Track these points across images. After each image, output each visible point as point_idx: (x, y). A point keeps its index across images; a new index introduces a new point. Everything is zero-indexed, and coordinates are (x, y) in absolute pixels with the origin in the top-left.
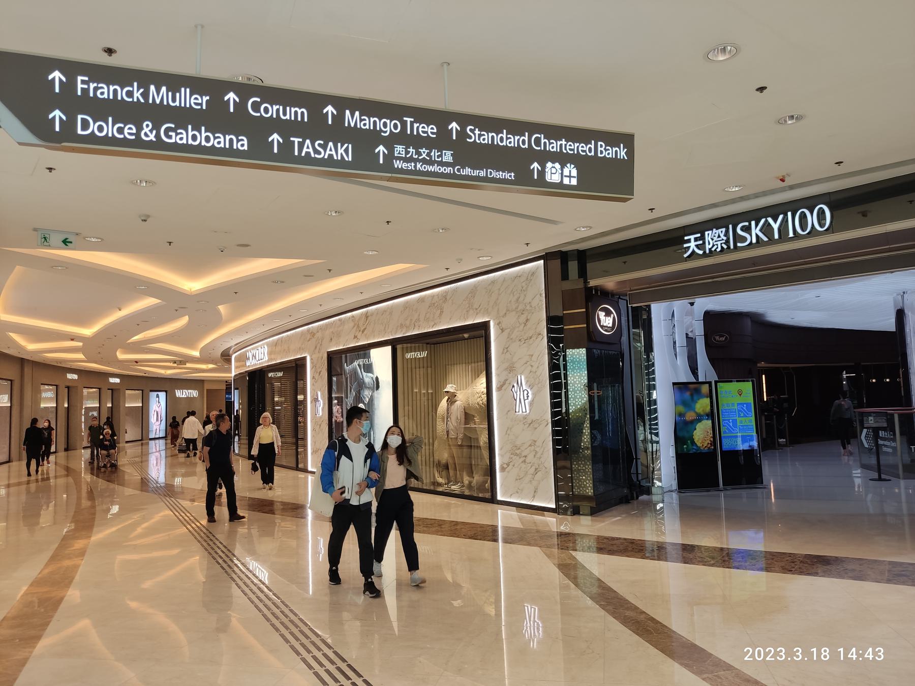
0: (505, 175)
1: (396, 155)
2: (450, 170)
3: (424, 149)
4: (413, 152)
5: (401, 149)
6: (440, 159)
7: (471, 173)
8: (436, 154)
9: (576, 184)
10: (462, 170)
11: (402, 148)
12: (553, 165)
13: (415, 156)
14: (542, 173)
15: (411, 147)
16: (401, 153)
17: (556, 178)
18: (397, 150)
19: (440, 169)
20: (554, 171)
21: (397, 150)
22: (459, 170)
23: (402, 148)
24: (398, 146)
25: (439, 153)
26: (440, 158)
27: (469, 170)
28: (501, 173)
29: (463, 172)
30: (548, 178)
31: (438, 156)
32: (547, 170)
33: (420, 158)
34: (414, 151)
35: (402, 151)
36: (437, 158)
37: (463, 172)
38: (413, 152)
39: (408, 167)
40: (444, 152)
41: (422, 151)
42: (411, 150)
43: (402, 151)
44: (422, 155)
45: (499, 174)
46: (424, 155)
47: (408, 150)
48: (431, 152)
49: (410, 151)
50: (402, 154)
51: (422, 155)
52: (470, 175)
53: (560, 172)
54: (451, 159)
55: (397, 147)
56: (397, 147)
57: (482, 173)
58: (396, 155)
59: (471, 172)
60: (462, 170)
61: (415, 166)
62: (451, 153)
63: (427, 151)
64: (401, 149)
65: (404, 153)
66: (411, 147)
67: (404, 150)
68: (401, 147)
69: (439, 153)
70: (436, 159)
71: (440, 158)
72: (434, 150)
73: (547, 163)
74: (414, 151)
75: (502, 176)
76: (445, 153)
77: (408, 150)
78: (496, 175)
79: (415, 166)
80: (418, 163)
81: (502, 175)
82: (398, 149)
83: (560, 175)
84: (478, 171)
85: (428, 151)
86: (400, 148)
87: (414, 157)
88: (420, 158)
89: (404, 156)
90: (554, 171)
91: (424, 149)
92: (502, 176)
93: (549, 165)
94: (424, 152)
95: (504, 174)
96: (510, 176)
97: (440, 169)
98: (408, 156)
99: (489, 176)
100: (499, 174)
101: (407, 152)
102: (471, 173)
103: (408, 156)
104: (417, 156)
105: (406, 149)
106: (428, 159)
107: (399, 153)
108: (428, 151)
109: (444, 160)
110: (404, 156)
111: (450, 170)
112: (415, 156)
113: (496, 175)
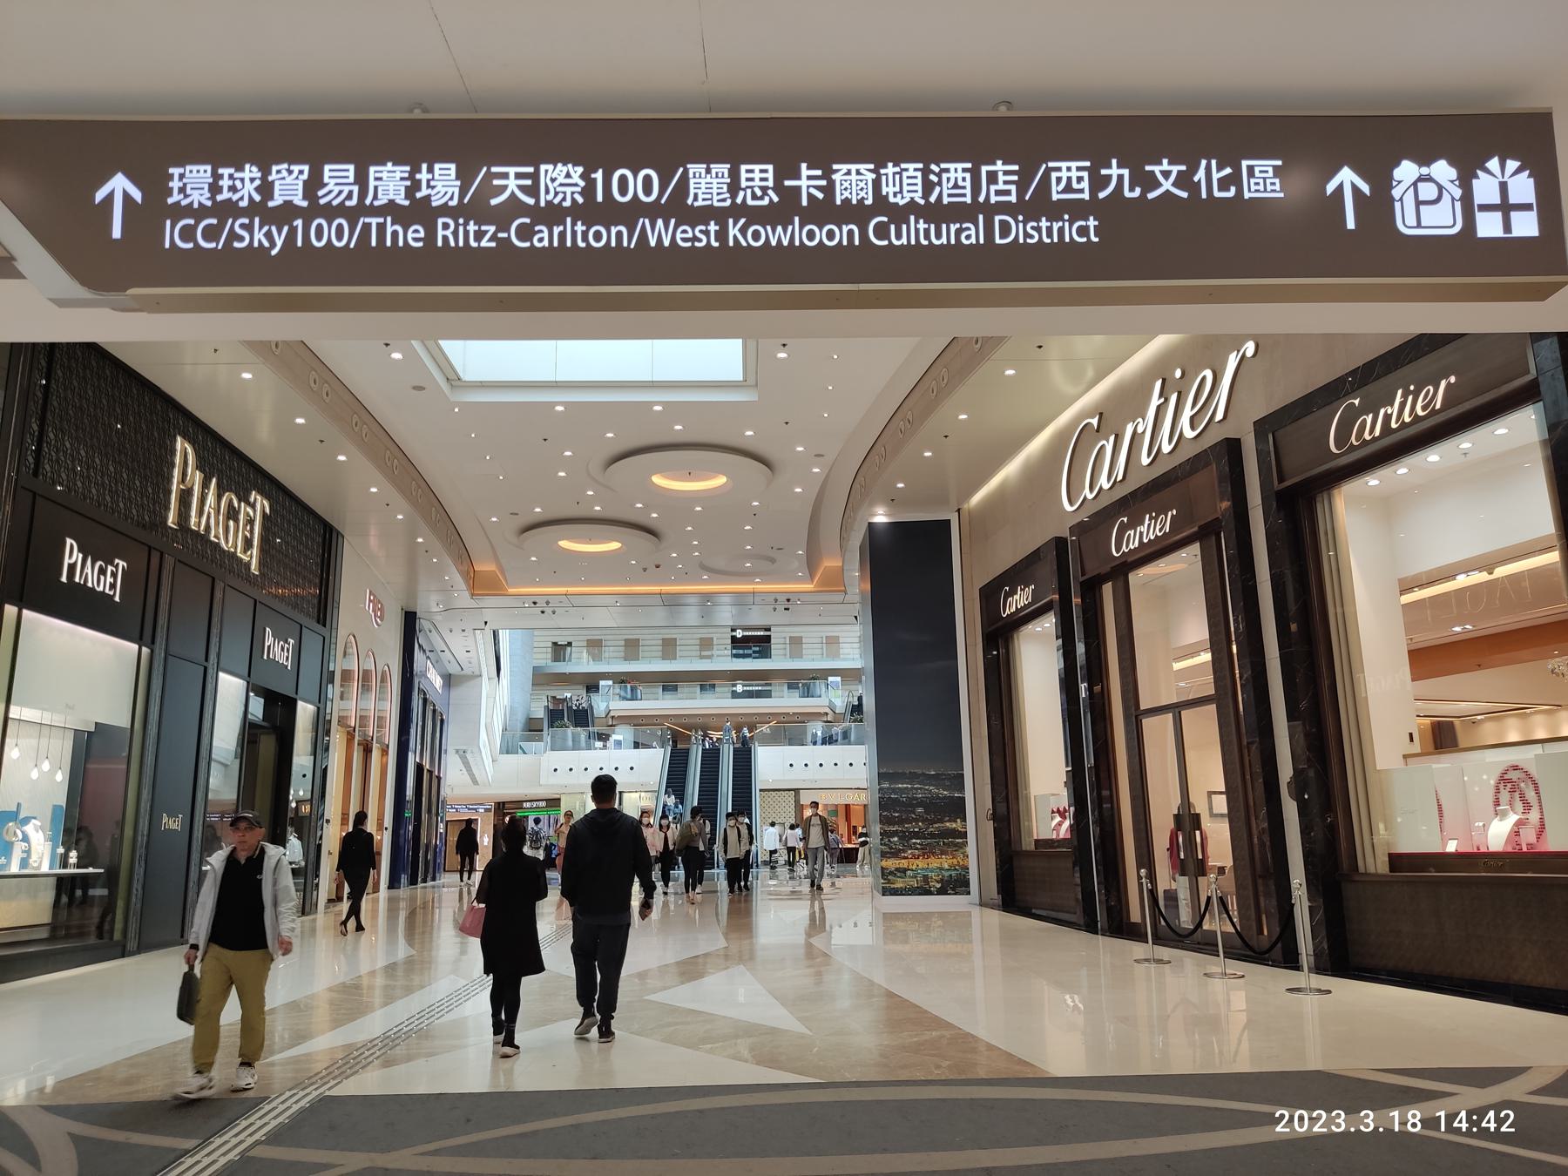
0: (1061, 230)
1: (1055, 197)
2: (850, 233)
3: (1165, 161)
4: (1120, 177)
5: (1074, 174)
6: (1232, 192)
7: (927, 236)
8: (1216, 176)
9: (1354, 228)
10: (893, 227)
11: (1079, 169)
12: (1425, 171)
13: (1132, 189)
14: (1378, 205)
15: (1114, 162)
16: (960, 183)
17: (1442, 220)
18: (948, 179)
19: (811, 235)
20: (1428, 192)
21: (1059, 180)
22: (881, 231)
23: (1079, 169)
24: (1064, 165)
25: (1228, 171)
26: (1233, 189)
27: (922, 226)
28: (1044, 224)
29: (899, 237)
30: (1406, 222)
31: (1224, 184)
32: (1396, 193)
33: (1151, 196)
34: (1126, 172)
35: (1080, 179)
36: (1220, 189)
37: (899, 237)
38: (1120, 177)
39: (695, 239)
40: (1245, 163)
41: (1156, 169)
42: (1114, 171)
43: (1080, 179)
44: (1160, 185)
45: (1038, 229)
46: (1167, 185)
47: (1104, 172)
48: (1193, 169)
49: (1109, 177)
50: (1081, 191)
51: (1160, 185)
52: (925, 243)
53: (1458, 193)
54: (1277, 187)
55: (1059, 169)
56: (1059, 169)
57: (973, 232)
58: (1055, 197)
59: (927, 232)
60: (893, 227)
61: (722, 235)
62: (1274, 167)
63: (1175, 169)
64: (960, 175)
65: (1085, 185)
66: (1114, 162)
67: (1085, 174)
68: (1074, 165)
69: (1228, 171)
70: (1217, 194)
71: (1233, 189)
72: (1204, 162)
73: (1398, 164)
74: (1126, 172)
75: (1050, 235)
76: (1251, 169)
77: (1104, 172)
78: (1027, 235)
79: (722, 235)
80: (731, 221)
81: (1049, 230)
82: (1064, 174)
83: (1458, 205)
84: (953, 228)
85: (1183, 168)
86: (858, 173)
87: (1127, 194)
88: (1151, 196)
89: (1086, 196)
90: (1428, 192)
91: (1165, 161)
92: (1050, 235)
93: (1406, 171)
94: (1166, 174)
95: (1056, 226)
96: (1083, 231)
97: (811, 235)
98: (1102, 195)
99: (998, 241)
100: (1038, 229)
101: (1098, 182)
102: (927, 236)
103: (1102, 195)
104: (1137, 192)
105: (1093, 172)
106: (1184, 195)
107: (1068, 188)
108: (1183, 168)
109: (1247, 195)
110: (1086, 196)
111: (850, 233)
112: (1132, 189)
113: (1027, 235)
